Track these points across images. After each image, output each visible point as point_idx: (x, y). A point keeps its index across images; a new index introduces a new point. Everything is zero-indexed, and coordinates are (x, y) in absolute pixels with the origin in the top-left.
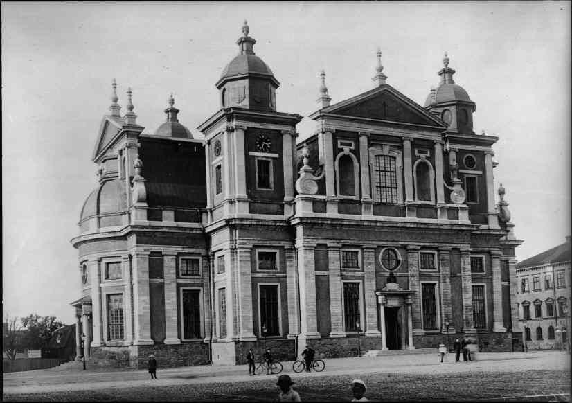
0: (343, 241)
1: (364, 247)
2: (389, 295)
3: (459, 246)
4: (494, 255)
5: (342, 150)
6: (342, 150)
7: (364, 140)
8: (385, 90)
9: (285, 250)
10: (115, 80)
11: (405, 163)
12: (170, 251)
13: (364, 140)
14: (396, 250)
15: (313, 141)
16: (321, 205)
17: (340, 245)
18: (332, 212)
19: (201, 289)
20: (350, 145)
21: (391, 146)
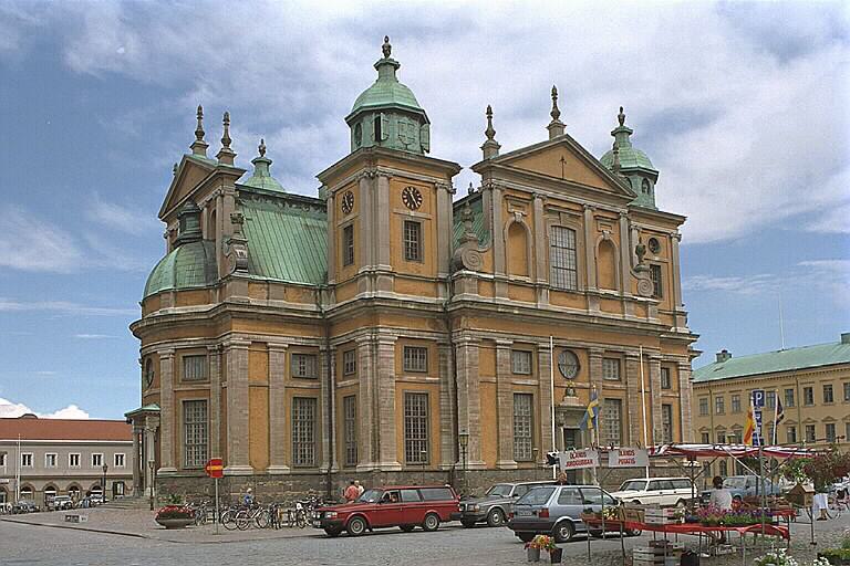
12: (282, 339)
15: (474, 197)
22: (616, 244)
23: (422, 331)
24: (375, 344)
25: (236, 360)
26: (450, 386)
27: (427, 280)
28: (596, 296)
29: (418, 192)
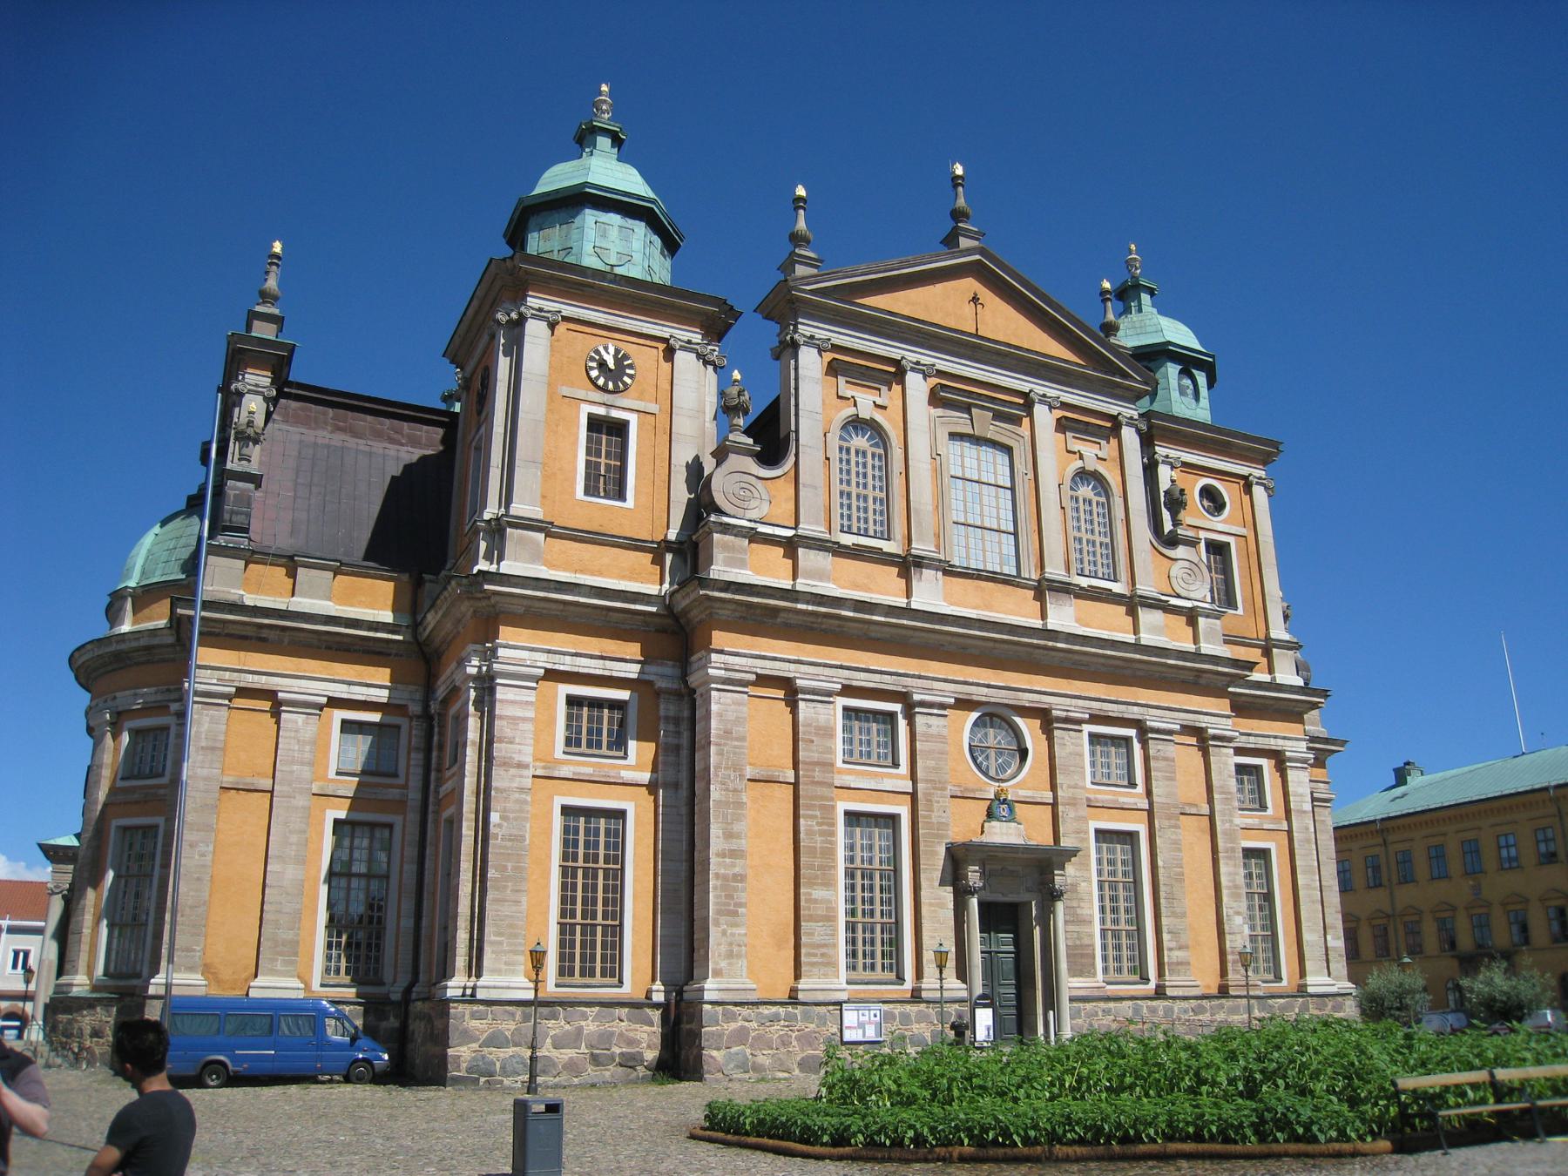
0: (846, 673)
2: (995, 859)
3: (1203, 721)
4: (1291, 759)
9: (658, 693)
14: (1019, 720)
19: (397, 820)
22: (1113, 478)
23: (626, 661)
24: (487, 685)
25: (204, 724)
26: (684, 793)
27: (635, 545)
28: (1065, 589)
29: (626, 357)
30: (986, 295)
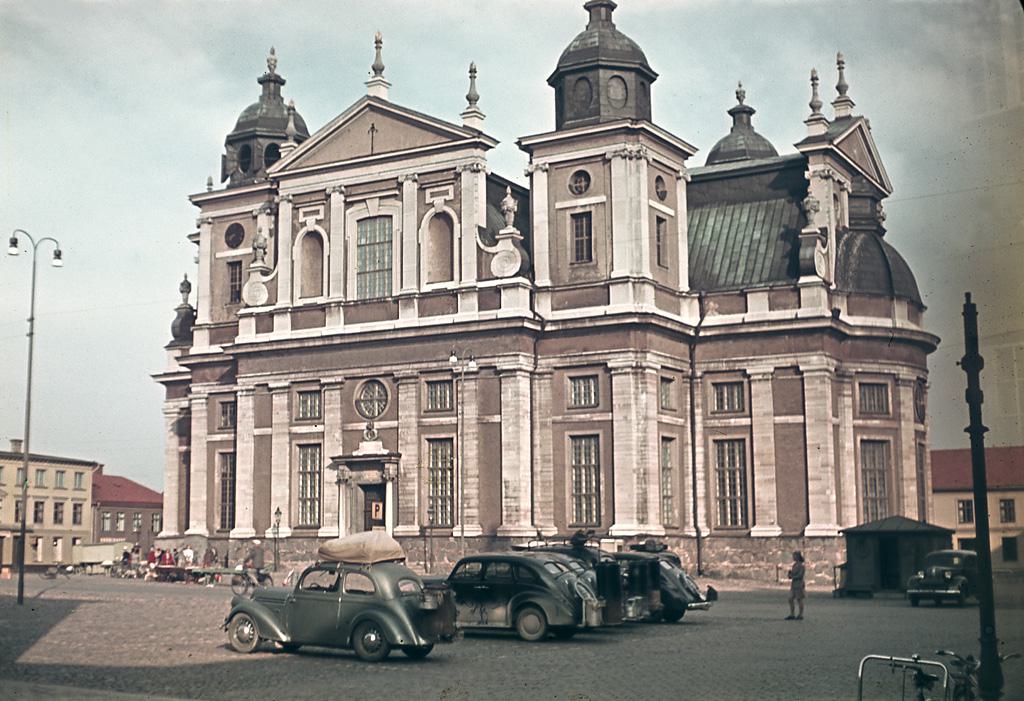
0: (293, 376)
1: (323, 381)
5: (304, 224)
6: (304, 224)
7: (337, 199)
8: (369, 105)
10: (814, 72)
11: (408, 221)
13: (337, 199)
14: (381, 380)
16: (267, 321)
17: (286, 384)
18: (283, 329)
20: (317, 212)
21: (381, 198)
30: (377, 118)
